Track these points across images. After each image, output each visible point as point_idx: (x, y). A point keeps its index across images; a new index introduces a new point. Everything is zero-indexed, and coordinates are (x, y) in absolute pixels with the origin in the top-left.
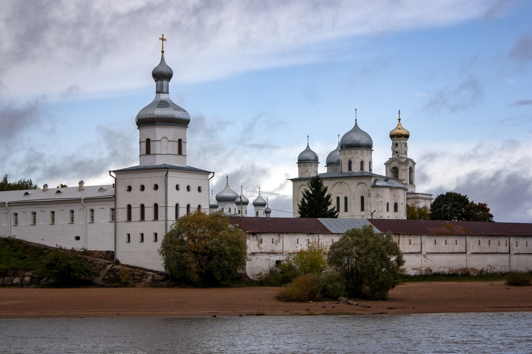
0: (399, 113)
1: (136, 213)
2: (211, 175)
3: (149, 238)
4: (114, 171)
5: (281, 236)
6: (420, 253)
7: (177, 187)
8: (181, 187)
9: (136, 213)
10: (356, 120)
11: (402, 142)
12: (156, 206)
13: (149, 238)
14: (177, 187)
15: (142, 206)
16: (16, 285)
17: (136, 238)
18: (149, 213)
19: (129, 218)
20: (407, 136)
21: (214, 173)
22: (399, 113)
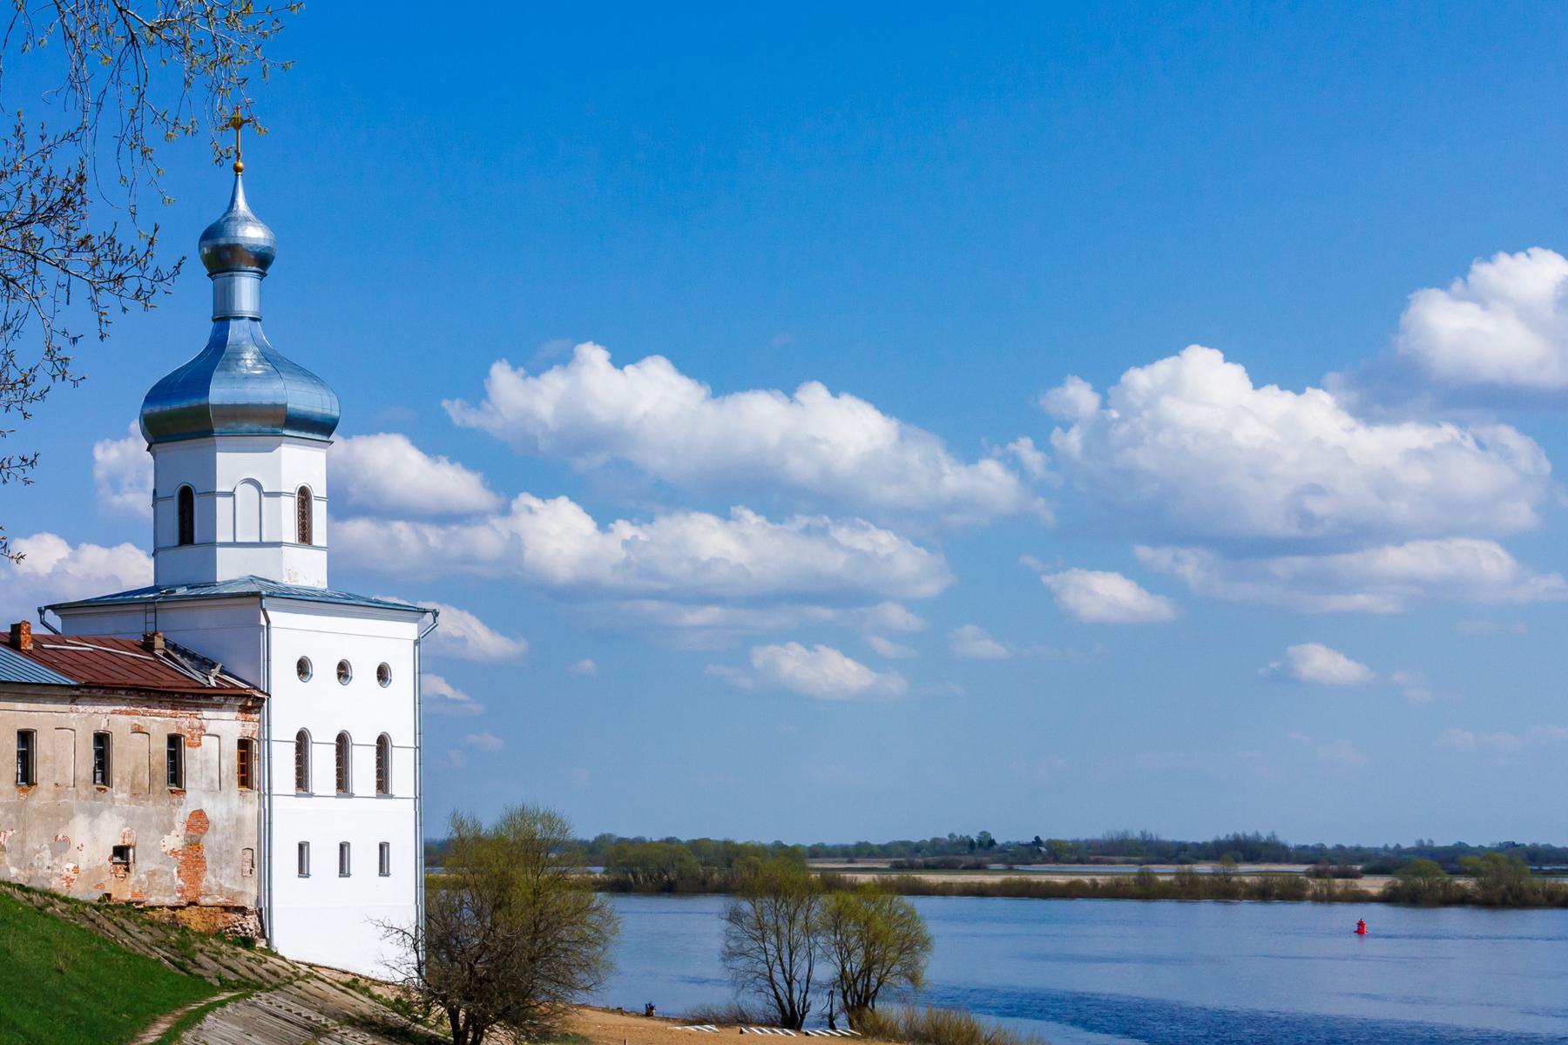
7: (303, 668)
8: (355, 671)
12: (382, 744)
14: (303, 668)
15: (342, 742)
17: (324, 860)
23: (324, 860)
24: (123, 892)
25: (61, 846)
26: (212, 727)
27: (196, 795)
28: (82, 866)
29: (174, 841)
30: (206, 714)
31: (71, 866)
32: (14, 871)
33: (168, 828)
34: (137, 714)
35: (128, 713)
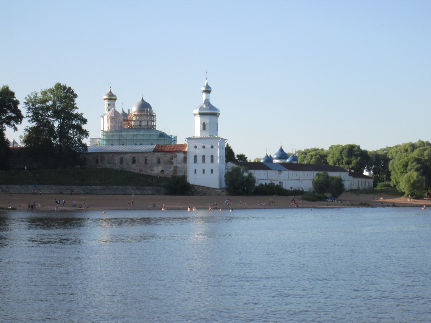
0: (110, 83)
1: (200, 159)
2: (226, 140)
3: (208, 171)
4: (187, 138)
5: (255, 170)
6: (300, 180)
9: (200, 159)
10: (142, 95)
11: (112, 103)
13: (208, 171)
16: (149, 194)
17: (200, 171)
18: (208, 159)
19: (196, 161)
20: (115, 99)
21: (227, 140)
22: (110, 83)
23: (200, 171)
24: (163, 175)
25: (152, 170)
26: (179, 155)
27: (175, 164)
28: (156, 173)
29: (172, 169)
30: (177, 154)
31: (154, 173)
32: (145, 173)
33: (171, 168)
34: (165, 154)
35: (163, 154)
